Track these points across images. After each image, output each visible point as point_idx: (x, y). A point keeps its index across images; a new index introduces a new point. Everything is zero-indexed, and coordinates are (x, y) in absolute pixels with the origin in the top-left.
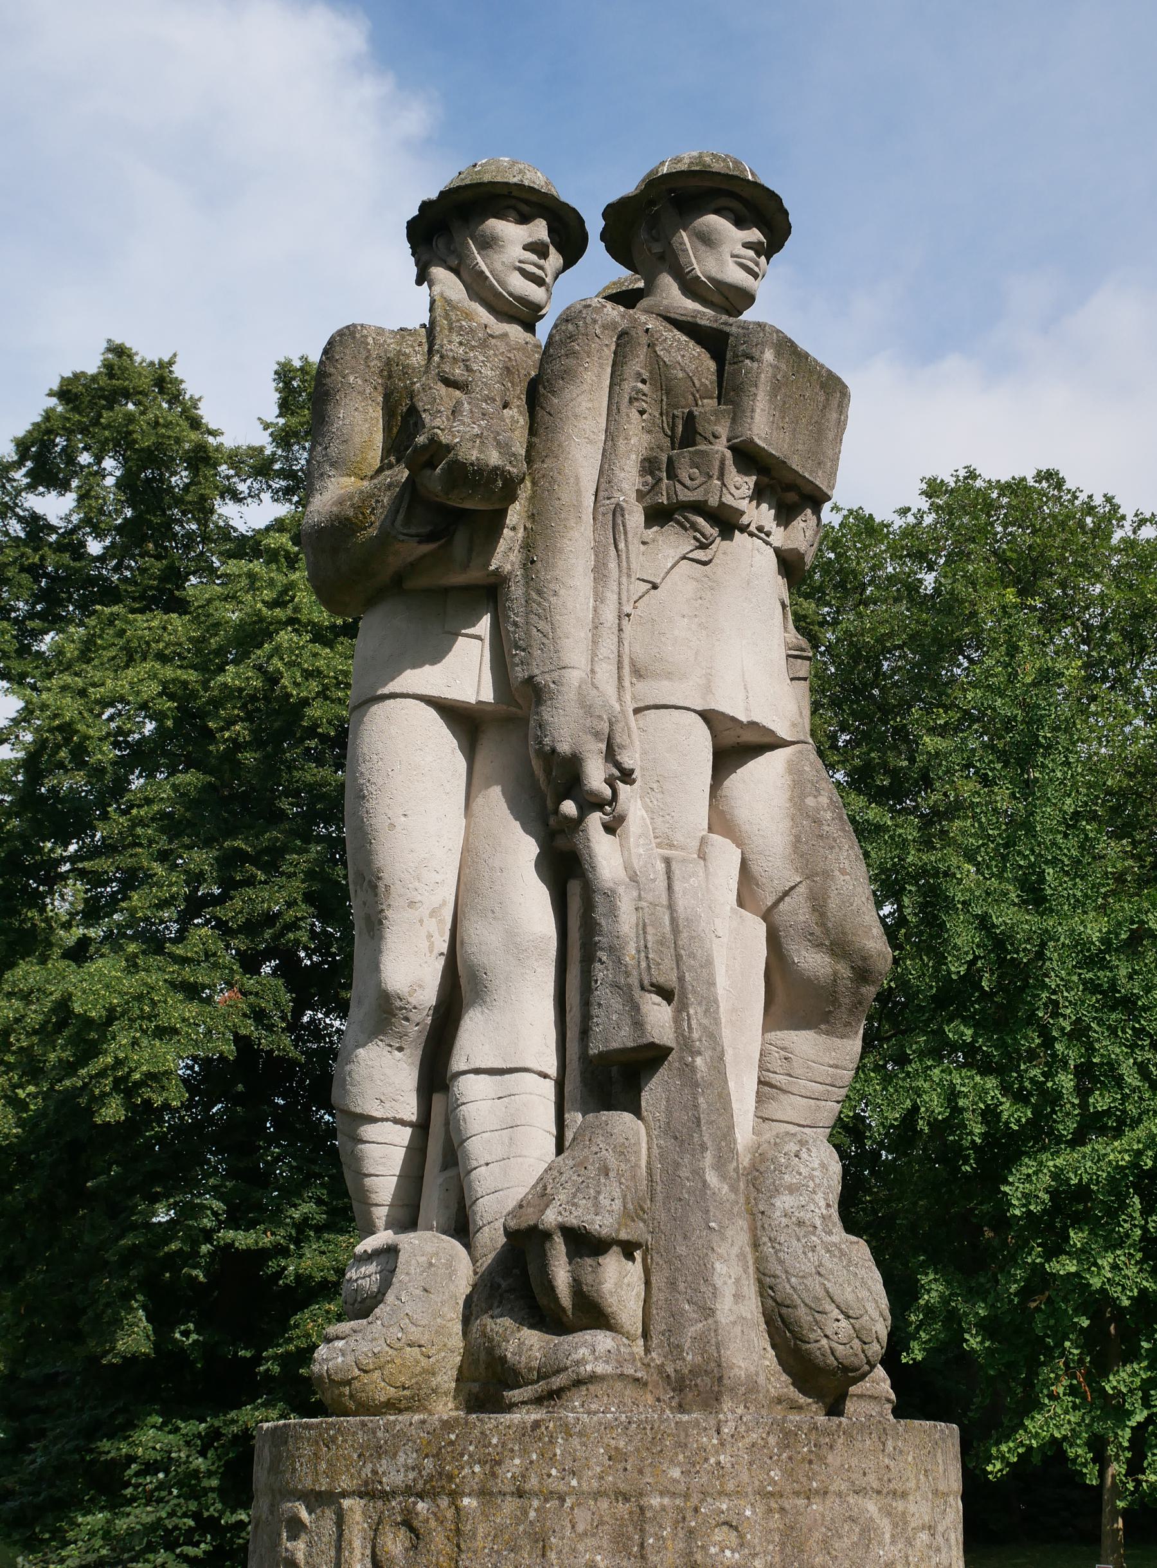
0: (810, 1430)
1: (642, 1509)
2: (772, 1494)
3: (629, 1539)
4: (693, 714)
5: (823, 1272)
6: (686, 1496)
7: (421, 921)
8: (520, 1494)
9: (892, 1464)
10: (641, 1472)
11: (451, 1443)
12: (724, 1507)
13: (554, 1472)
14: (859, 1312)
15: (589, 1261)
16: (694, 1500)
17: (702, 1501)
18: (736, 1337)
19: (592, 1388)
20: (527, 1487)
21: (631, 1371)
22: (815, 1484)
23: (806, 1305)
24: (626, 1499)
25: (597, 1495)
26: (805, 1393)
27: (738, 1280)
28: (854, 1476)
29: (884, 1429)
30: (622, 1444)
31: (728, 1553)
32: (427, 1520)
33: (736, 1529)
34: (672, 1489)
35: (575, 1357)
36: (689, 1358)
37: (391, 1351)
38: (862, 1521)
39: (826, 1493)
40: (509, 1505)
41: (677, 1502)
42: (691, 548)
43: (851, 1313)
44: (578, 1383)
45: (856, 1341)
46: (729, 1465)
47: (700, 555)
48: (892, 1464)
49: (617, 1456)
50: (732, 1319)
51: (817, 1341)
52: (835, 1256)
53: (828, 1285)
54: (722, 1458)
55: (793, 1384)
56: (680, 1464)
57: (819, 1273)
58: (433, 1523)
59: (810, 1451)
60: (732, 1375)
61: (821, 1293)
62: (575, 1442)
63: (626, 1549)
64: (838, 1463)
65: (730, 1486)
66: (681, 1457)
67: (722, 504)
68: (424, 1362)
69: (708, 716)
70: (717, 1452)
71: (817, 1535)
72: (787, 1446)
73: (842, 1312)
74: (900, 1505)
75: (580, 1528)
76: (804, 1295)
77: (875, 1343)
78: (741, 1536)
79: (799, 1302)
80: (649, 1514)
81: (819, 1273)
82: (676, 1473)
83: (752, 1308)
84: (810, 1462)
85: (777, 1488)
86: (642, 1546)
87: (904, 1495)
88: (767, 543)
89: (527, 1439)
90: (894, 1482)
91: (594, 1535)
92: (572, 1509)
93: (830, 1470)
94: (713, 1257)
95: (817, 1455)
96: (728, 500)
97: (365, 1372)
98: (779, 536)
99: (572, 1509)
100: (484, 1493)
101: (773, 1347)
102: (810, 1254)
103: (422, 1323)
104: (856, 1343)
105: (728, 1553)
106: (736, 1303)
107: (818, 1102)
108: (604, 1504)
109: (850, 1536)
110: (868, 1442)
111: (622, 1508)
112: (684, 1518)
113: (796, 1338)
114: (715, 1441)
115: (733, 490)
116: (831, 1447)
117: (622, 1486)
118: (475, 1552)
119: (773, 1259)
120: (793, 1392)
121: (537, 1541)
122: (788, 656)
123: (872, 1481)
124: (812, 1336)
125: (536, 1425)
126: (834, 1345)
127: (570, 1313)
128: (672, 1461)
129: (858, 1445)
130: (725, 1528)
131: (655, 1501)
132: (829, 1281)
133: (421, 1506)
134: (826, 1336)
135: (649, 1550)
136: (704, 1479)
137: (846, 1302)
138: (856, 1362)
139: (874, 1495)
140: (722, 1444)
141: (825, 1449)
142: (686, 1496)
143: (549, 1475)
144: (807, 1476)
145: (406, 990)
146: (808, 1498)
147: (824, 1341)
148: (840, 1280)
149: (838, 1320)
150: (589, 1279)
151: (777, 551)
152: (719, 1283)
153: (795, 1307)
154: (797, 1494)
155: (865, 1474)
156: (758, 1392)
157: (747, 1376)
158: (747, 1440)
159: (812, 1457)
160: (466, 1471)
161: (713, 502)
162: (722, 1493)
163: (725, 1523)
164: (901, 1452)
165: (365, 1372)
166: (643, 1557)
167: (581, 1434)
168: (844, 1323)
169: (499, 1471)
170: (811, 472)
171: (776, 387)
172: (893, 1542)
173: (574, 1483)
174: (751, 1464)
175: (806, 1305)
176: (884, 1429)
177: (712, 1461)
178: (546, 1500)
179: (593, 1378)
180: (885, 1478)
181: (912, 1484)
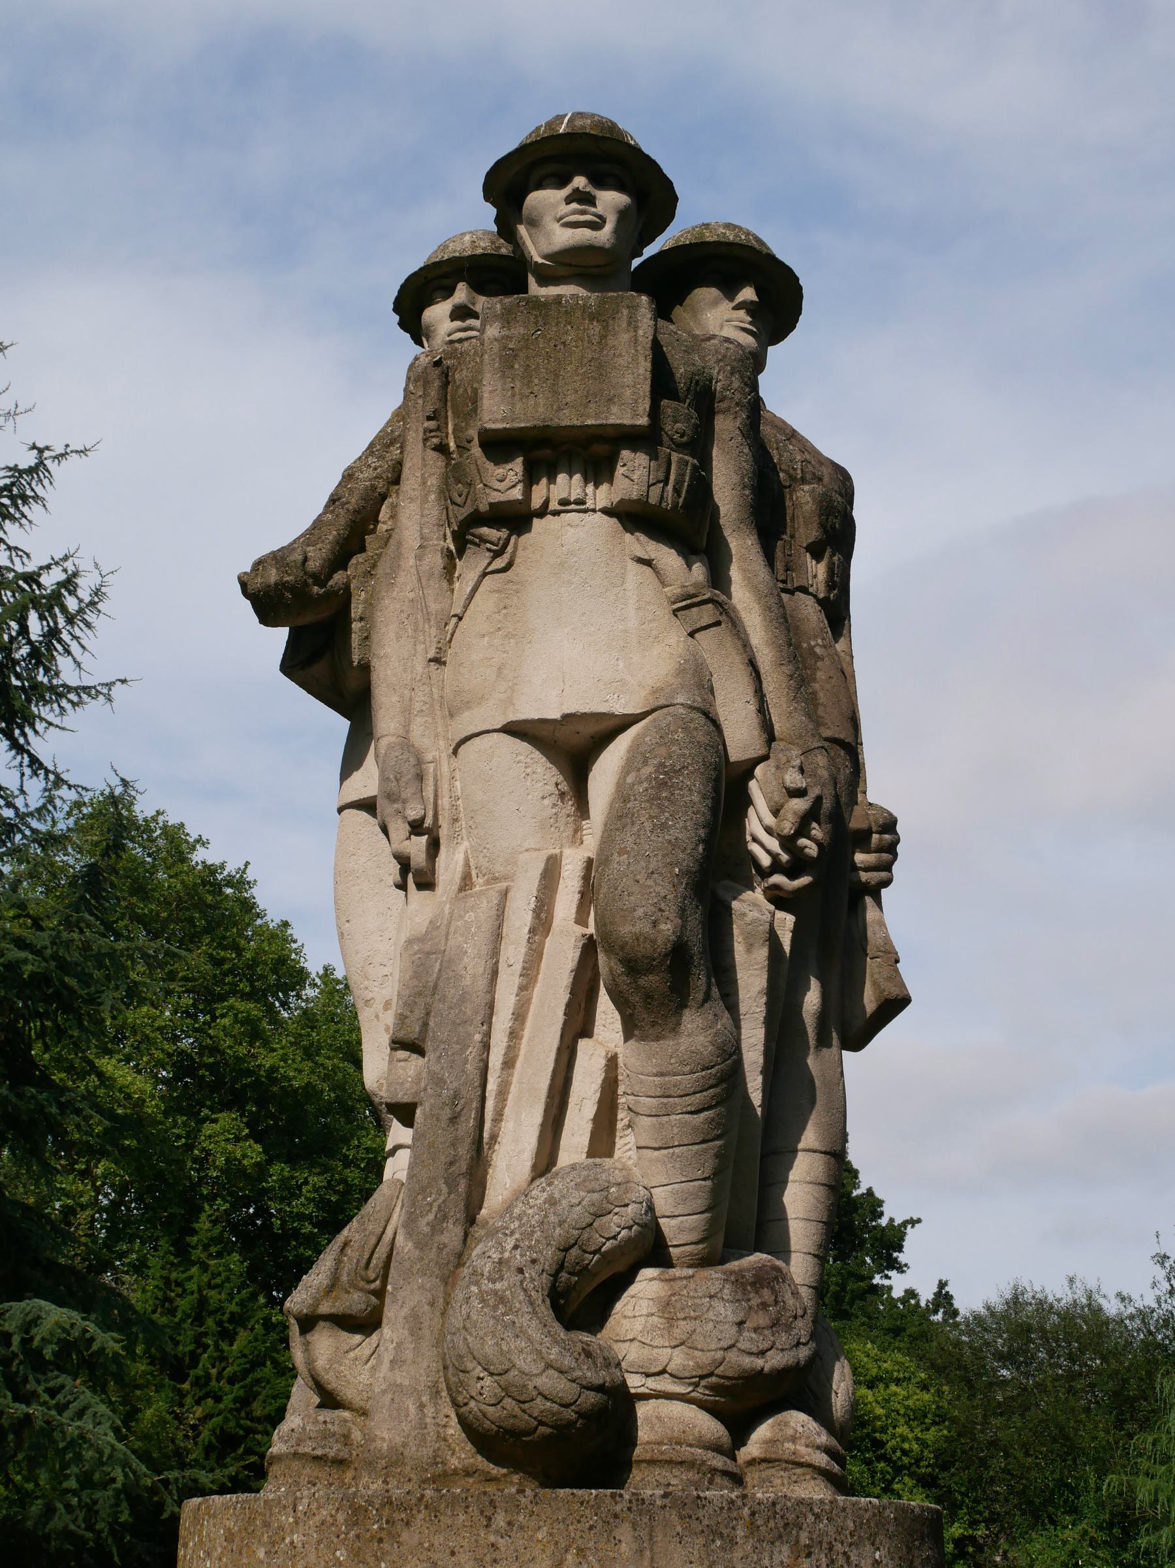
0: (383, 1506)
4: (495, 734)
7: (377, 1017)
9: (502, 1542)
14: (501, 1368)
21: (308, 1450)
26: (497, 1464)
27: (399, 1345)
28: (435, 1556)
42: (487, 561)
45: (510, 1400)
46: (300, 1545)
47: (499, 563)
48: (502, 1542)
50: (383, 1387)
51: (466, 1404)
52: (488, 1306)
53: (470, 1339)
56: (264, 1545)
57: (464, 1327)
59: (381, 1529)
60: (372, 1448)
67: (491, 504)
69: (514, 730)
70: (292, 1532)
72: (356, 1524)
77: (539, 1400)
84: (380, 1541)
88: (585, 511)
93: (404, 1549)
95: (389, 1533)
96: (496, 497)
98: (602, 496)
104: (508, 1402)
106: (392, 1369)
107: (659, 1119)
110: (462, 1517)
114: (291, 1520)
115: (497, 485)
116: (408, 1524)
120: (481, 1462)
122: (675, 612)
128: (259, 1541)
129: (445, 1520)
132: (471, 1334)
138: (522, 1425)
140: (296, 1523)
141: (399, 1525)
144: (375, 1556)
145: (375, 1085)
147: (472, 1404)
151: (606, 511)
155: (453, 1553)
157: (390, 1448)
158: (317, 1518)
161: (483, 507)
164: (521, 1528)
168: (488, 1381)
170: (597, 416)
174: (319, 1542)
176: (492, 1502)
177: (287, 1540)
180: (488, 1558)
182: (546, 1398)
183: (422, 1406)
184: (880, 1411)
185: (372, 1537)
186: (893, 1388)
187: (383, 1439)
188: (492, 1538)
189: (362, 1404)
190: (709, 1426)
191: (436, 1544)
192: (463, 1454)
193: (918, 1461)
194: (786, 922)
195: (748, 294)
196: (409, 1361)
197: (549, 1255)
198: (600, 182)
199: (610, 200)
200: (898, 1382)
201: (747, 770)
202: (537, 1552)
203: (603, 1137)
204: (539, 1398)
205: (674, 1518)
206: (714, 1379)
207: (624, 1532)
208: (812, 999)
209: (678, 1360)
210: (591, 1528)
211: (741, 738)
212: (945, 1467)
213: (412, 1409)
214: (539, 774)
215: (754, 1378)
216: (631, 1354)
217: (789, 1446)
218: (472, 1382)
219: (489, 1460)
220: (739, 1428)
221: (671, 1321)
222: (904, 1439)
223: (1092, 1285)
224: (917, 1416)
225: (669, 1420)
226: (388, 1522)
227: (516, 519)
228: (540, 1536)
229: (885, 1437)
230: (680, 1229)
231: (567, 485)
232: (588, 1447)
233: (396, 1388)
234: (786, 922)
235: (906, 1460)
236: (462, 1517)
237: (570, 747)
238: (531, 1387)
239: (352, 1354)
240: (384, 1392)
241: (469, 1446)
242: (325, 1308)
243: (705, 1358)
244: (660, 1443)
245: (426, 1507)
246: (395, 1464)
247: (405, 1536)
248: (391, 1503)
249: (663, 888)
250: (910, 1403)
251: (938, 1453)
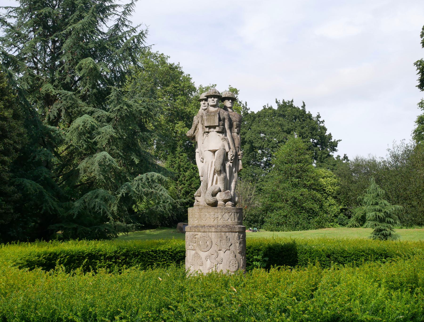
98: (215, 130)
171: (207, 120)
184: (325, 183)
186: (328, 178)
190: (223, 203)
192: (206, 205)
193: (333, 193)
194: (231, 164)
195: (230, 101)
197: (211, 192)
198: (214, 98)
199: (216, 99)
200: (329, 177)
201: (228, 152)
203: (216, 183)
208: (234, 170)
209: (221, 199)
211: (227, 150)
212: (339, 194)
214: (211, 154)
215: (226, 200)
216: (218, 198)
220: (225, 203)
222: (330, 189)
223: (374, 155)
224: (333, 184)
225: (220, 203)
227: (208, 132)
229: (326, 189)
230: (222, 189)
231: (212, 130)
232: (215, 204)
234: (231, 164)
235: (330, 193)
237: (214, 152)
249: (219, 166)
250: (331, 181)
251: (337, 192)
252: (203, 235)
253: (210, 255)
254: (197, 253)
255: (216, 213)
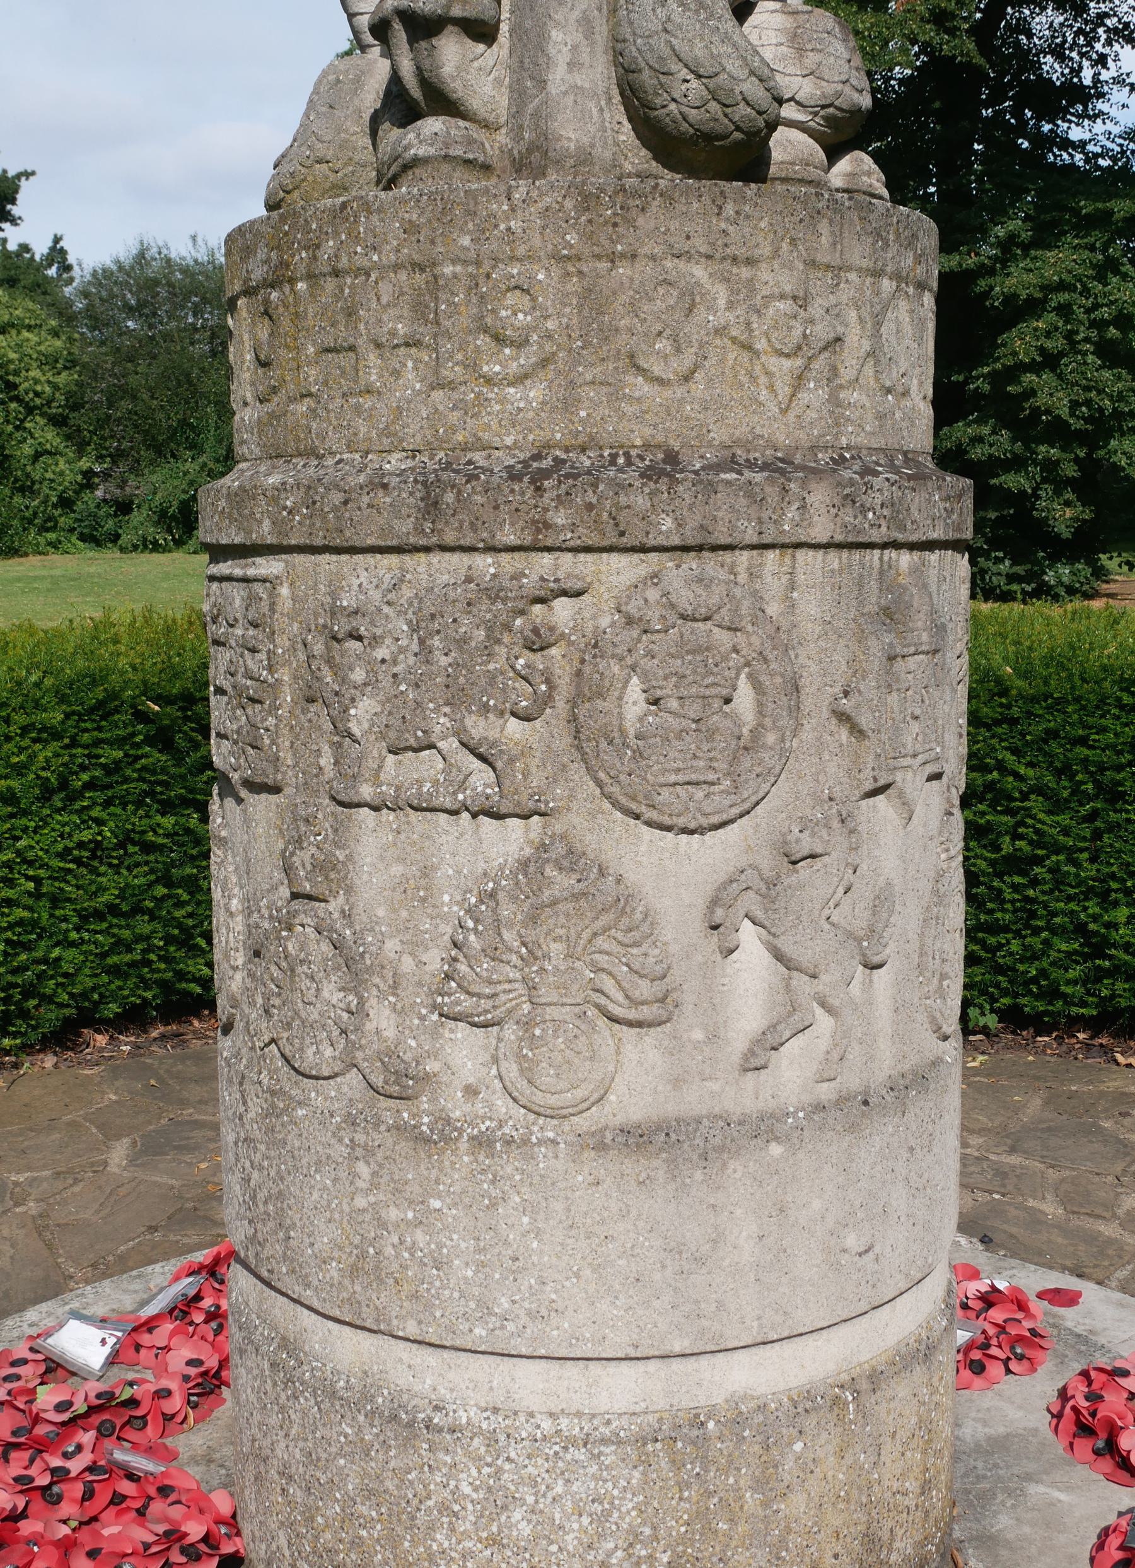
0: (616, 193)
1: (436, 278)
2: (568, 258)
3: (427, 307)
5: (669, 27)
6: (478, 263)
8: (336, 273)
9: (731, 229)
10: (433, 242)
11: (286, 234)
12: (515, 271)
13: (359, 249)
14: (711, 71)
15: (424, 44)
16: (486, 267)
17: (494, 267)
18: (566, 108)
19: (417, 171)
20: (340, 266)
21: (460, 153)
22: (619, 247)
23: (650, 67)
24: (422, 270)
25: (397, 267)
27: (575, 48)
28: (671, 240)
29: (722, 192)
30: (415, 217)
31: (521, 316)
32: (277, 308)
33: (527, 292)
34: (463, 257)
35: (405, 142)
36: (527, 136)
37: (303, 170)
38: (682, 284)
39: (634, 256)
40: (330, 284)
41: (470, 269)
43: (702, 71)
44: (406, 168)
45: (714, 103)
46: (519, 230)
48: (731, 229)
49: (410, 229)
50: (563, 88)
51: (664, 107)
52: (689, 10)
53: (674, 41)
54: (513, 223)
55: (655, 158)
56: (469, 232)
57: (666, 30)
58: (281, 309)
59: (615, 214)
61: (666, 52)
62: (375, 218)
63: (424, 316)
64: (652, 225)
65: (521, 251)
66: (470, 225)
68: (332, 177)
70: (508, 219)
71: (623, 298)
72: (588, 209)
73: (692, 72)
74: (745, 272)
75: (384, 301)
76: (649, 56)
77: (742, 105)
78: (534, 299)
79: (643, 65)
80: (441, 282)
81: (666, 30)
82: (466, 241)
83: (599, 74)
84: (615, 225)
85: (574, 252)
86: (436, 314)
87: (750, 262)
89: (338, 220)
90: (733, 247)
91: (395, 306)
92: (376, 283)
94: (550, 24)
95: (624, 218)
97: (288, 192)
99: (376, 283)
100: (310, 277)
101: (630, 120)
102: (659, 11)
103: (326, 139)
104: (713, 106)
105: (521, 316)
106: (570, 71)
108: (403, 276)
109: (663, 301)
110: (695, 205)
111: (420, 279)
112: (477, 285)
113: (643, 106)
114: (505, 208)
116: (643, 209)
117: (417, 257)
118: (307, 330)
119: (624, 23)
120: (655, 167)
121: (350, 315)
123: (699, 244)
124: (658, 101)
125: (344, 206)
126: (685, 109)
127: (423, 104)
128: (462, 230)
130: (517, 292)
131: (448, 270)
132: (676, 37)
133: (274, 295)
134: (674, 100)
135: (441, 315)
136: (494, 246)
137: (695, 58)
138: (719, 129)
139: (703, 260)
140: (513, 210)
141: (634, 212)
142: (478, 263)
143: (356, 253)
144: (611, 239)
146: (612, 261)
147: (673, 106)
148: (689, 35)
149: (688, 81)
150: (426, 64)
152: (552, 51)
153: (640, 71)
154: (598, 257)
155: (688, 237)
156: (592, 164)
157: (577, 148)
159: (618, 220)
160: (297, 257)
162: (513, 258)
163: (516, 287)
164: (748, 217)
165: (288, 192)
166: (437, 323)
167: (380, 211)
168: (694, 83)
169: (318, 253)
172: (727, 309)
173: (375, 258)
175: (650, 67)
176: (722, 192)
177: (502, 227)
178: (356, 277)
179: (416, 162)
180: (720, 242)
181: (767, 251)
182: (748, 104)
183: (601, 110)
184: (13, 356)
185: (606, 222)
186: (26, 334)
187: (569, 139)
188: (723, 225)
189: (487, 115)
190: (821, 154)
191: (672, 228)
193: (49, 404)
196: (587, 64)
200: (29, 328)
202: (760, 240)
204: (743, 104)
205: (856, 218)
206: (831, 110)
207: (824, 227)
210: (801, 221)
212: (75, 407)
213: (595, 112)
217: (865, 179)
218: (677, 84)
219: (664, 166)
221: (801, 51)
222: (36, 381)
224: (49, 361)
226: (622, 208)
228: (762, 225)
229: (17, 380)
233: (577, 89)
235: (38, 401)
236: (695, 205)
238: (737, 92)
239: (476, 64)
240: (565, 93)
241: (644, 152)
242: (457, 11)
243: (830, 89)
244: (793, 163)
245: (661, 195)
246: (583, 163)
247: (641, 221)
248: (625, 191)
250: (42, 348)
251: (69, 395)
252: (685, 597)
253: (767, 861)
254: (573, 858)
255: (820, 282)
